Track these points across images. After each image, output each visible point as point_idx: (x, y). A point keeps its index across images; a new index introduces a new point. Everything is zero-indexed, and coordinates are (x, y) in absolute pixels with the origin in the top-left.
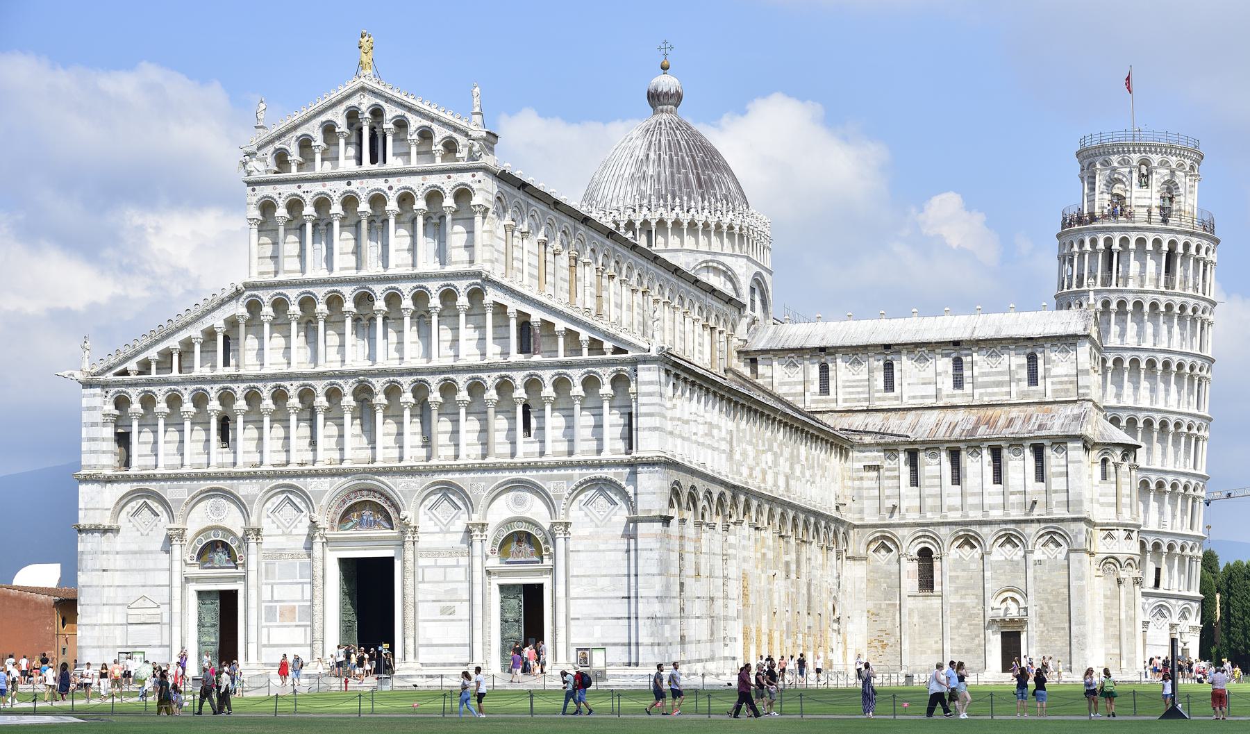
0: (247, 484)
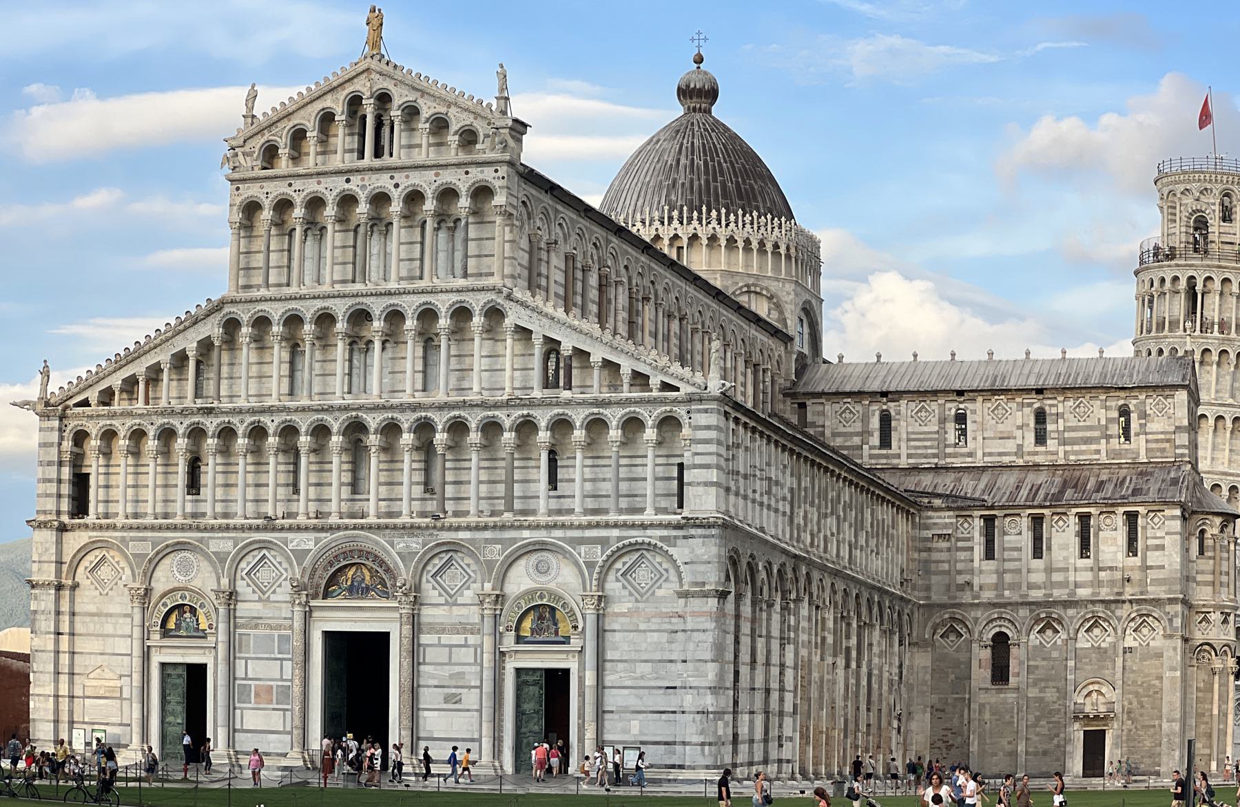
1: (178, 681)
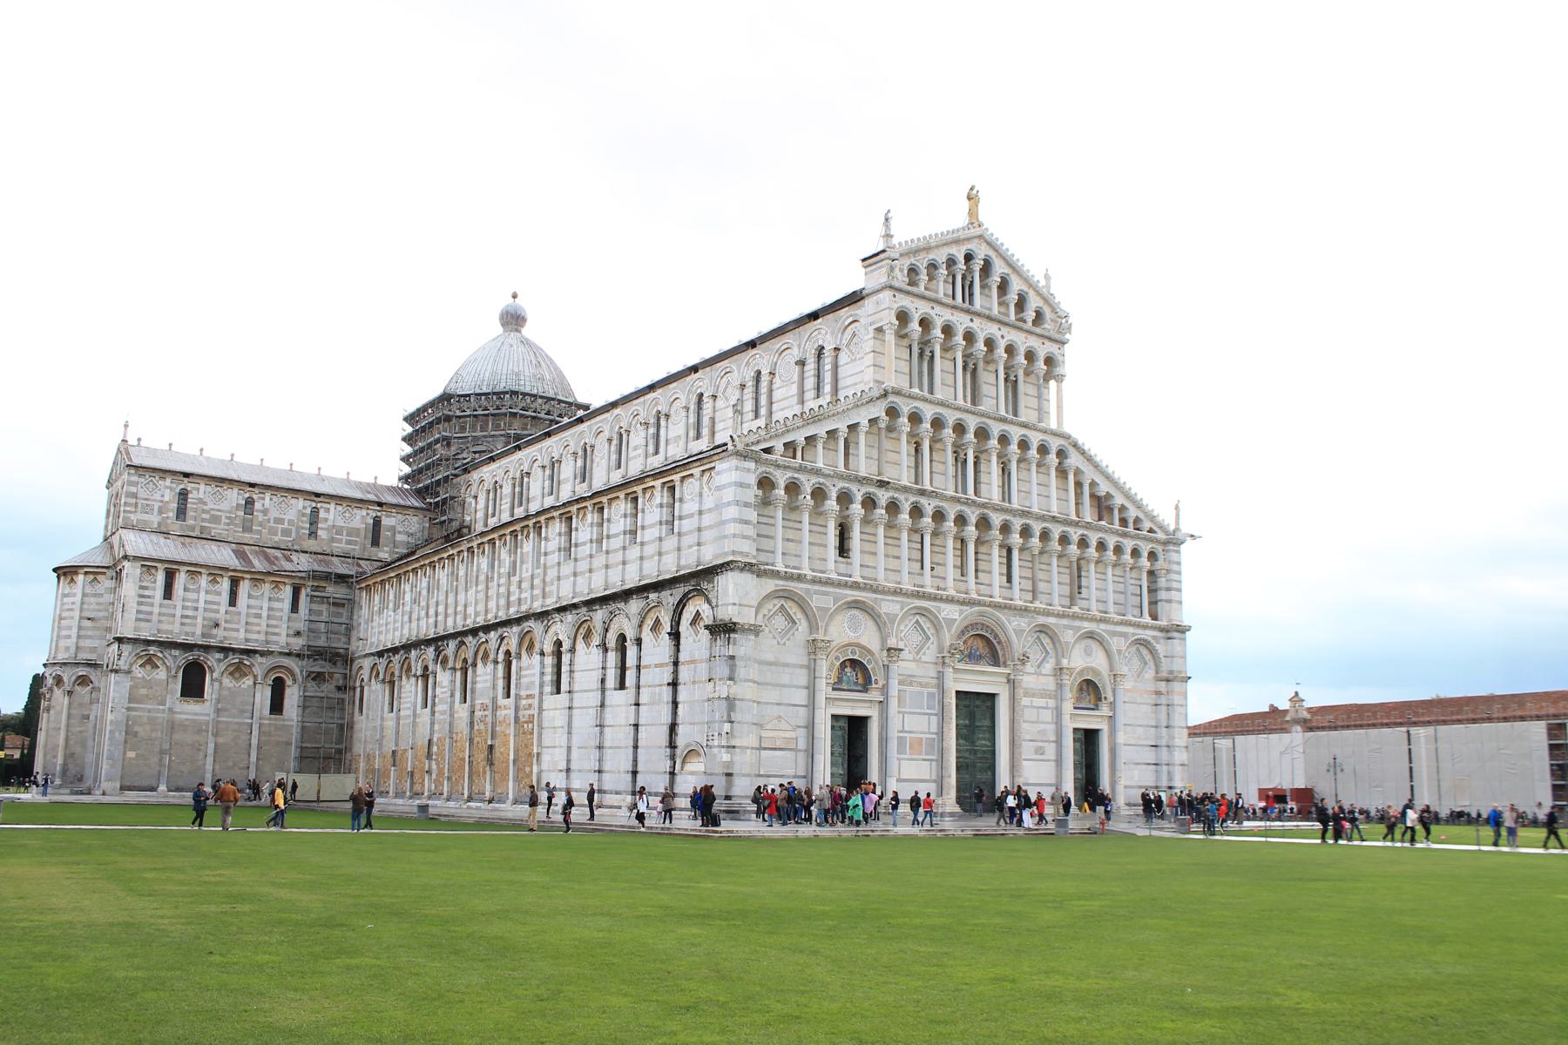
0: (888, 600)
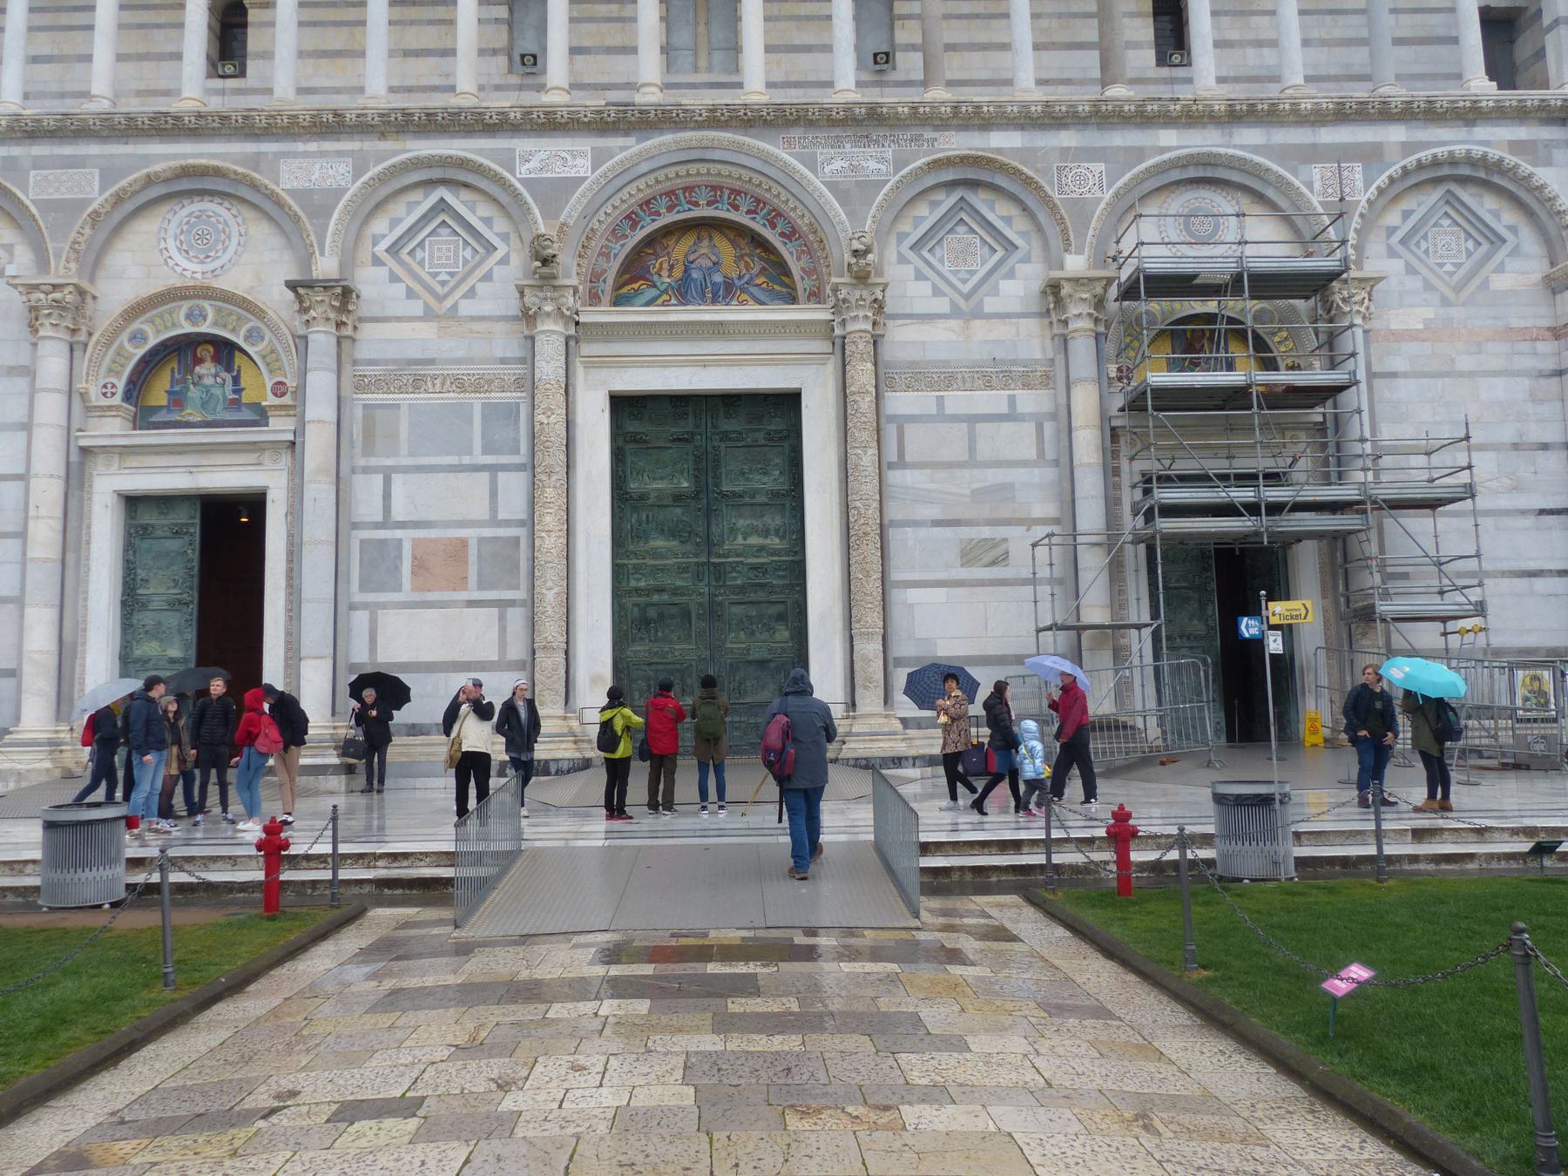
0: (306, 154)
1: (174, 545)
